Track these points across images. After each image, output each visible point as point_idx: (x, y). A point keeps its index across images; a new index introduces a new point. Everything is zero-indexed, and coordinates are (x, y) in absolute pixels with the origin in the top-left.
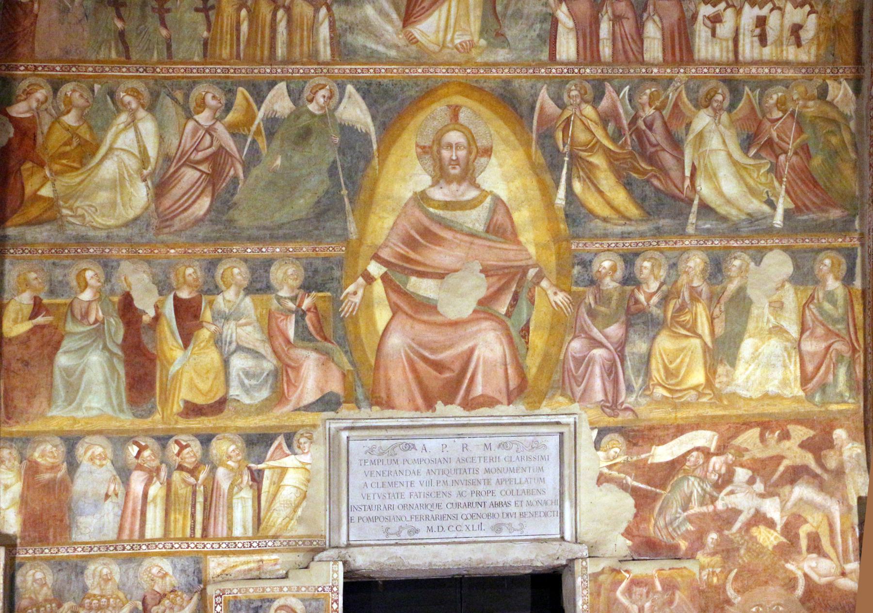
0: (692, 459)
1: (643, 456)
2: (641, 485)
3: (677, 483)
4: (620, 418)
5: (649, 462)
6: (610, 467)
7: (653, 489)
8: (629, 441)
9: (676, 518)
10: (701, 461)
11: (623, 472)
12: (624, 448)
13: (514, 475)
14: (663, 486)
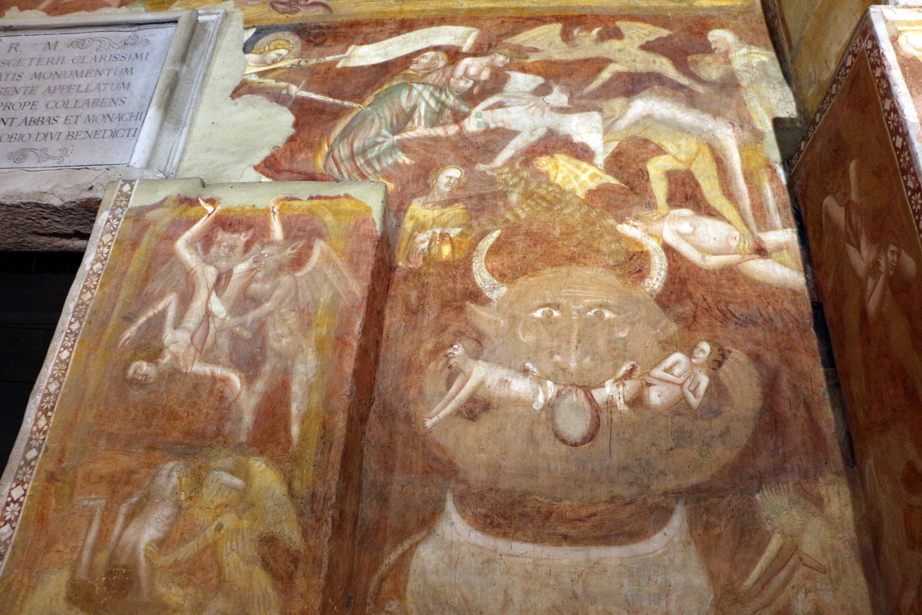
0: (424, 61)
1: (329, 59)
2: (313, 96)
3: (389, 92)
4: (299, 15)
5: (339, 66)
6: (261, 74)
7: (338, 101)
8: (309, 41)
9: (376, 144)
10: (441, 64)
11: (286, 80)
12: (297, 49)
13: (77, 81)
14: (358, 97)
